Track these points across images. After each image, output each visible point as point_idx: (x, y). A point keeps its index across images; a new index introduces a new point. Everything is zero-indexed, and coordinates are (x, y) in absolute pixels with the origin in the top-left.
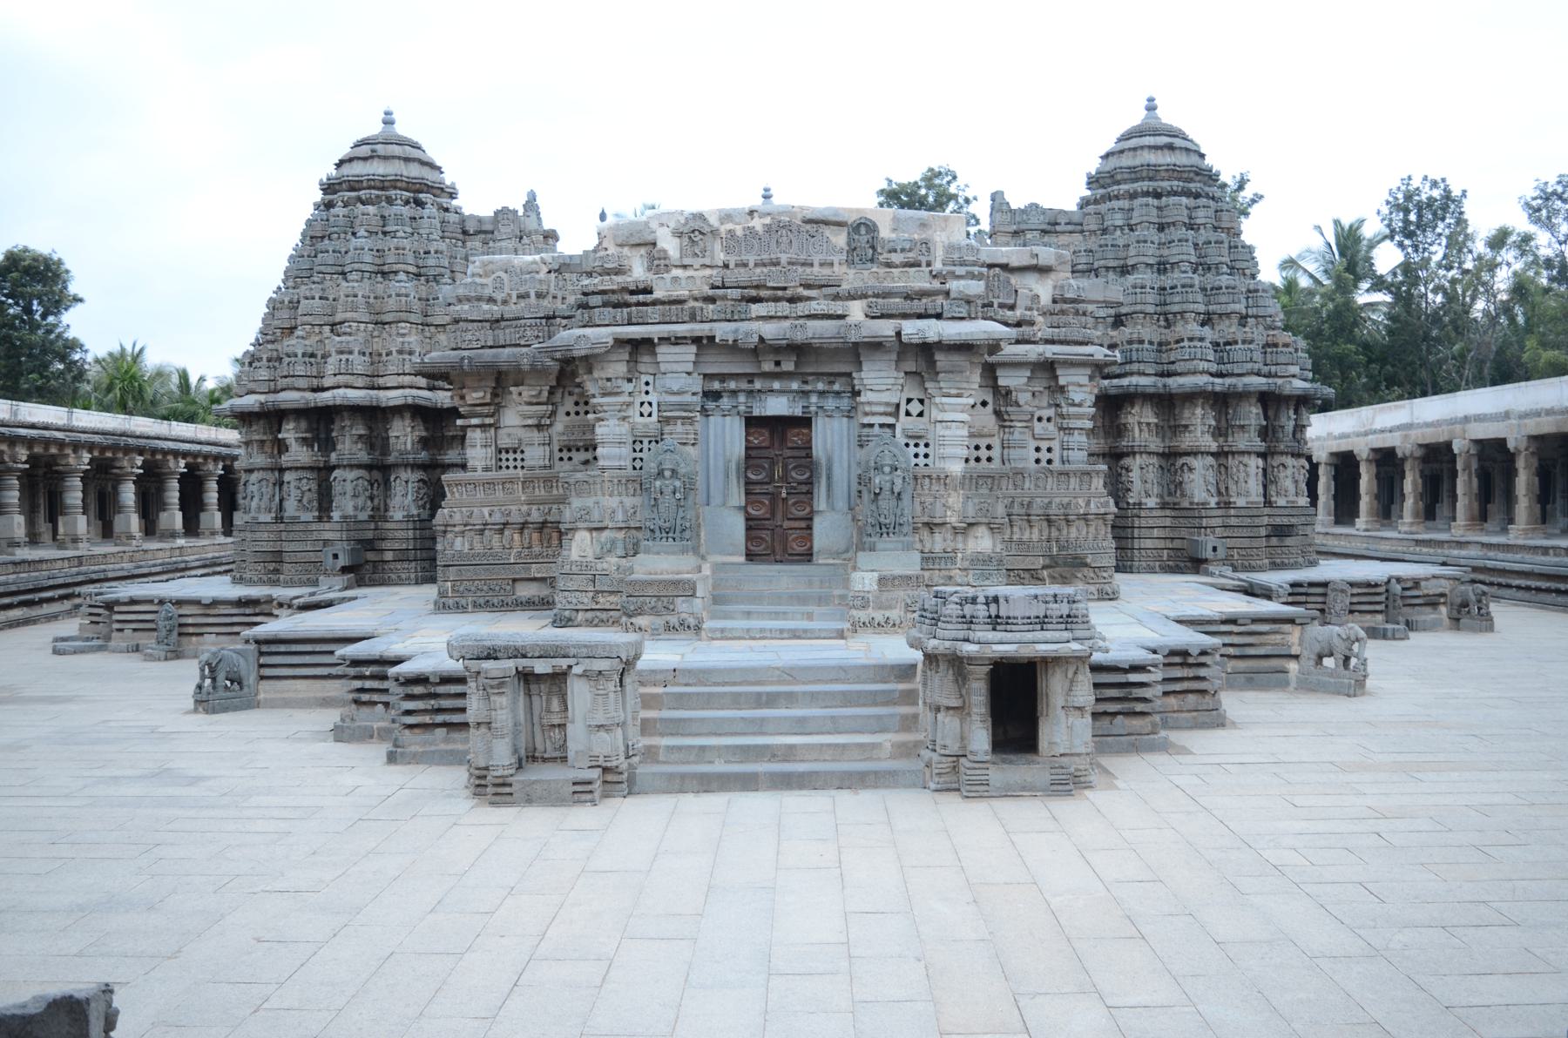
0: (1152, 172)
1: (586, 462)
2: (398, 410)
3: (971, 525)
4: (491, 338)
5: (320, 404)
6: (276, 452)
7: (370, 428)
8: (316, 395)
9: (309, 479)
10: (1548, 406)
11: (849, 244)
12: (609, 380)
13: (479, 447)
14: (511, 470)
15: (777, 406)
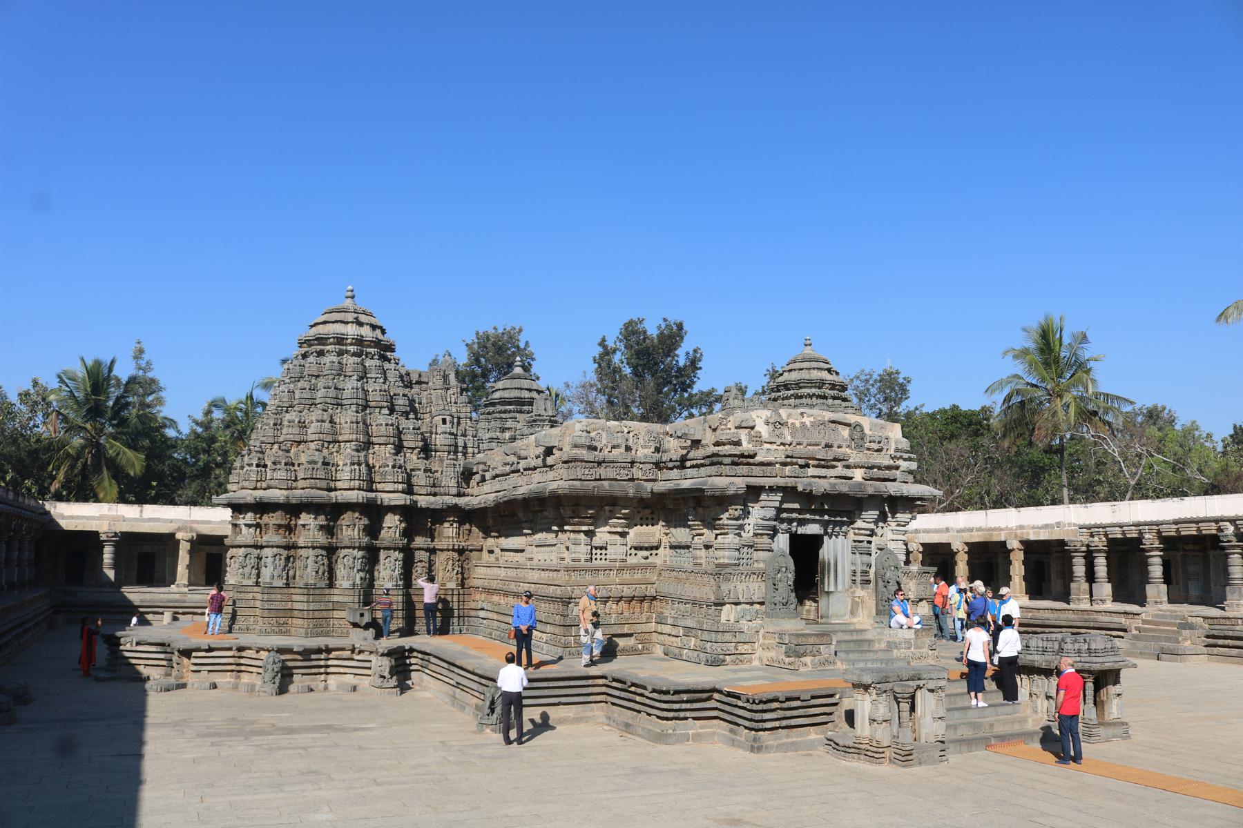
0: (821, 384)
1: (647, 558)
2: (393, 509)
3: (921, 600)
4: (598, 474)
5: (340, 501)
6: (287, 533)
7: (369, 520)
8: (338, 493)
9: (323, 556)
10: (978, 526)
11: (851, 436)
12: (736, 510)
13: (582, 545)
14: (603, 560)
15: (813, 529)
